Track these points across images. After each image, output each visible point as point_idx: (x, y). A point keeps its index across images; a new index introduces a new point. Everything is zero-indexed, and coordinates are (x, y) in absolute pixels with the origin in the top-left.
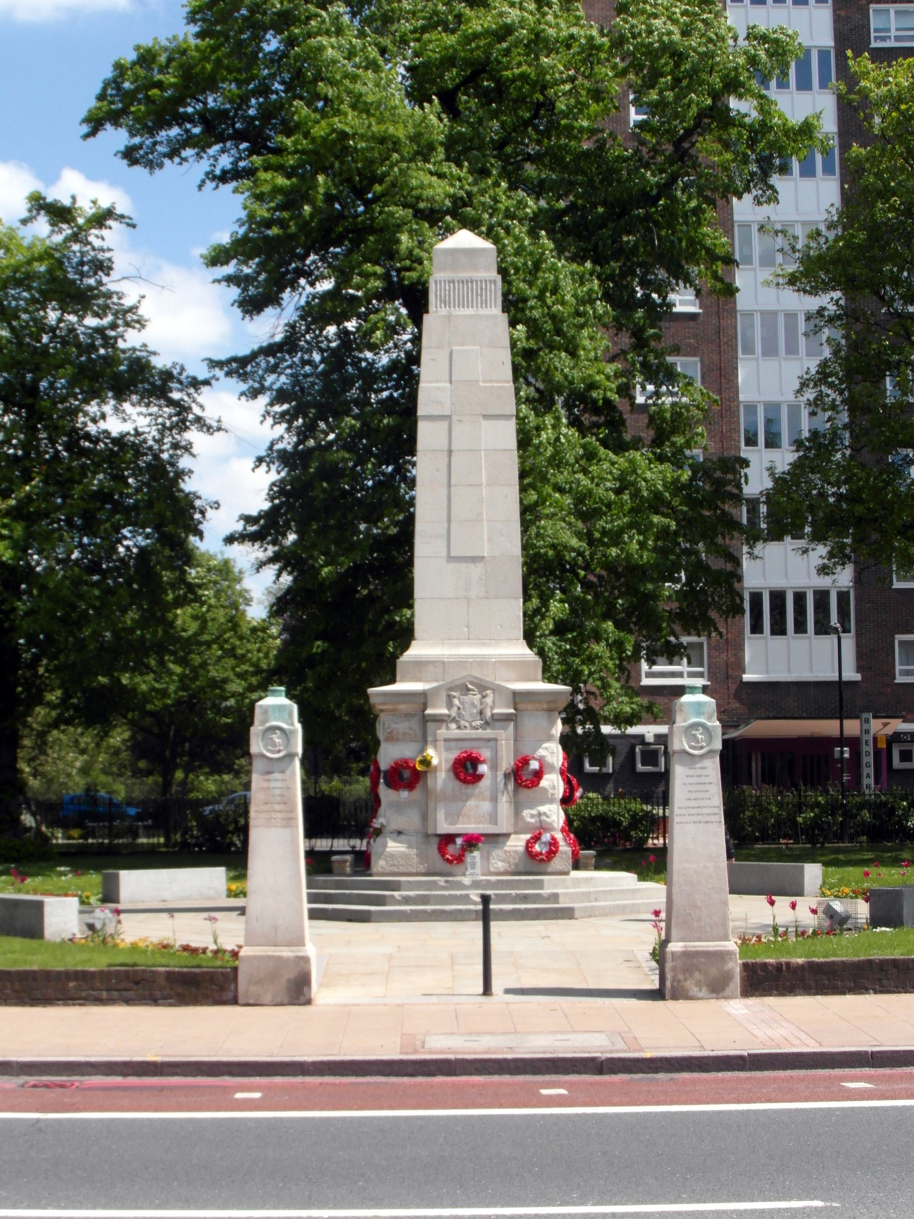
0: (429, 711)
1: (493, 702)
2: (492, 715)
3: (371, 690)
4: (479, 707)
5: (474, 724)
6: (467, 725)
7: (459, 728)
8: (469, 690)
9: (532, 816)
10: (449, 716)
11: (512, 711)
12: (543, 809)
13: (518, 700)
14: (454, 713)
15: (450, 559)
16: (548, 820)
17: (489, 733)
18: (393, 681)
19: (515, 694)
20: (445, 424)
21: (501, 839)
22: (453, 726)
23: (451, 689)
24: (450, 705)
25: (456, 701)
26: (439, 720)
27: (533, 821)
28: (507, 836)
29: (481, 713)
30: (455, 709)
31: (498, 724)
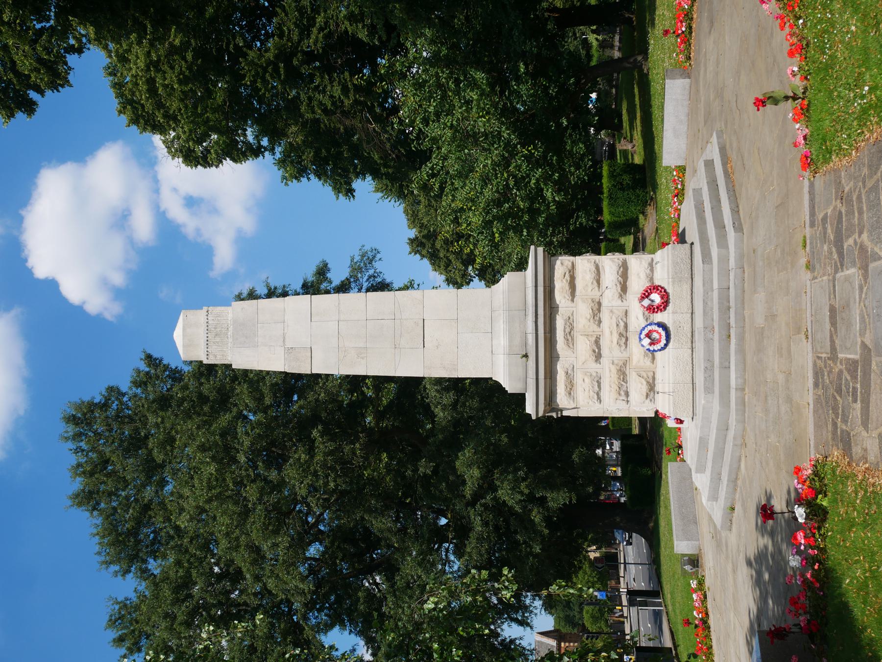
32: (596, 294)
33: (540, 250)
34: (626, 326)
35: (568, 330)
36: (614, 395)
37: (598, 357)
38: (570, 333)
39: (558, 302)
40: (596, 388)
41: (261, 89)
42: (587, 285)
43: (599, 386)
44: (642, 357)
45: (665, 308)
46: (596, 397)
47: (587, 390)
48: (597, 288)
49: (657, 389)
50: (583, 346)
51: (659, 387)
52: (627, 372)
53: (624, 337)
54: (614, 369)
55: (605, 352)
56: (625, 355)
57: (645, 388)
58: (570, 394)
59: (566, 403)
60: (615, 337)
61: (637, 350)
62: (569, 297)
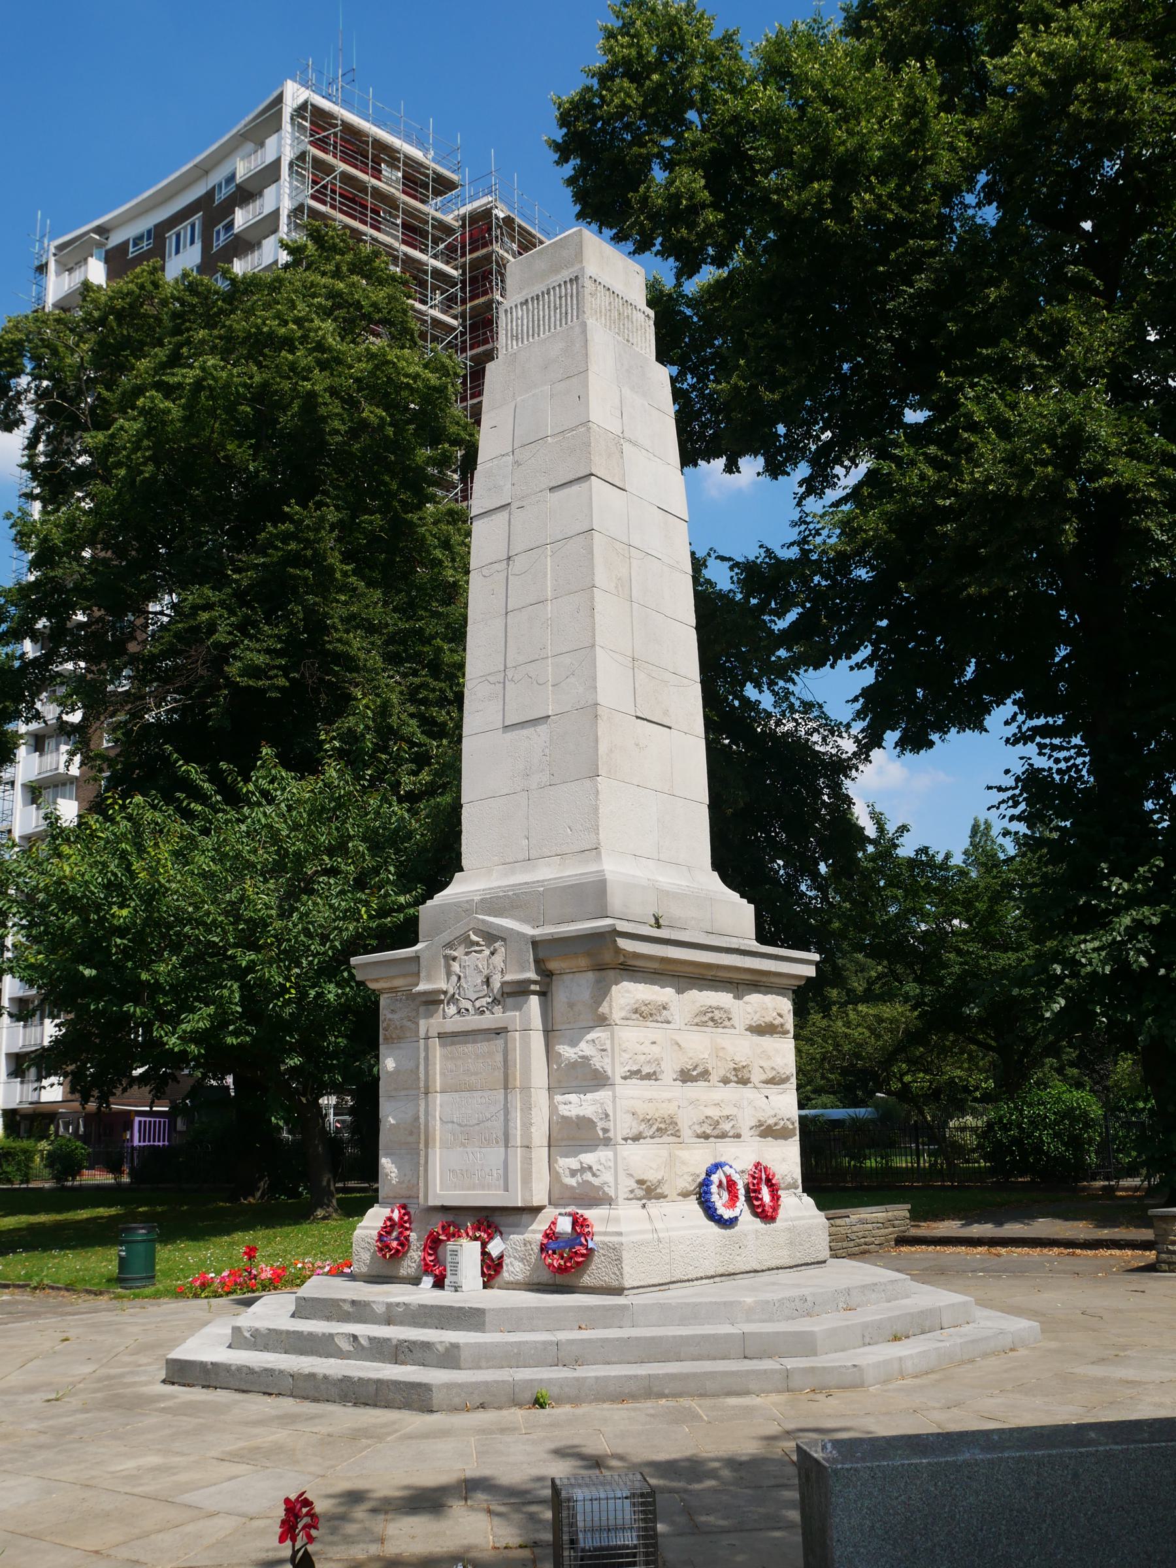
3: (354, 960)
4: (486, 972)
5: (478, 1004)
6: (469, 1005)
9: (573, 1173)
10: (445, 993)
12: (588, 1158)
15: (506, 728)
16: (596, 1182)
17: (496, 1017)
18: (415, 942)
19: (535, 944)
20: (504, 515)
21: (525, 1218)
22: (452, 1010)
23: (450, 945)
24: (449, 974)
25: (456, 967)
26: (432, 1001)
27: (572, 1182)
28: (537, 1210)
29: (487, 982)
32: (757, 1076)
33: (811, 972)
34: (723, 1136)
35: (717, 1015)
36: (642, 1108)
37: (686, 1077)
38: (712, 1019)
39: (747, 998)
40: (646, 1070)
41: (275, 527)
42: (769, 1058)
43: (648, 1076)
44: (692, 1170)
45: (756, 1214)
46: (635, 1068)
47: (642, 1048)
48: (764, 1077)
49: (649, 1204)
50: (699, 1046)
51: (654, 1207)
52: (666, 1139)
53: (713, 1132)
54: (671, 1109)
55: (695, 1090)
56: (686, 1133)
57: (651, 1176)
58: (636, 1011)
59: (622, 1001)
60: (715, 1113)
61: (696, 1159)
62: (757, 1020)
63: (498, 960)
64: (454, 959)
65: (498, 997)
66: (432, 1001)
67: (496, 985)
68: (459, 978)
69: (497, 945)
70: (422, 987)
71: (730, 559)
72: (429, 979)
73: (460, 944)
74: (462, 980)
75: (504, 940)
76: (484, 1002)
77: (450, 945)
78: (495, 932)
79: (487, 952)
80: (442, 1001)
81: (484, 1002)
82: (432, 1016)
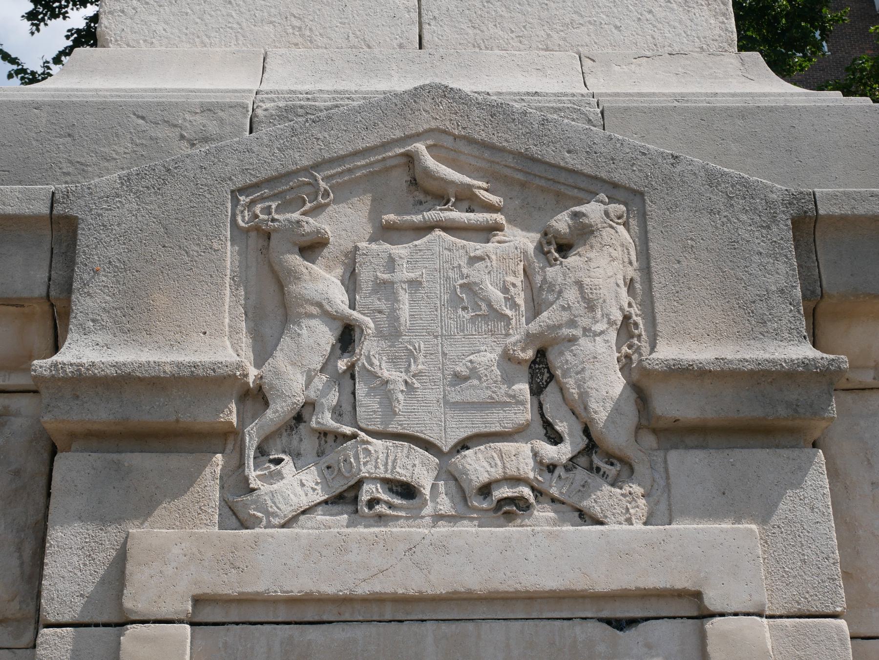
0: (80, 352)
1: (643, 285)
2: (641, 387)
4: (520, 327)
5: (479, 465)
6: (419, 469)
7: (346, 498)
8: (427, 191)
10: (256, 397)
11: (805, 351)
13: (833, 280)
14: (297, 369)
22: (296, 484)
24: (273, 310)
25: (323, 282)
29: (541, 369)
30: (324, 336)
31: (689, 465)
63: (605, 267)
64: (311, 248)
65: (618, 438)
66: (163, 430)
67: (601, 382)
68: (347, 337)
69: (593, 210)
70: (80, 352)
71: (13, 61)
72: (129, 321)
73: (343, 191)
74: (370, 349)
75: (615, 190)
76: (521, 457)
77: (289, 186)
78: (571, 161)
79: (521, 240)
80: (226, 438)
81: (521, 457)
82: (144, 510)
